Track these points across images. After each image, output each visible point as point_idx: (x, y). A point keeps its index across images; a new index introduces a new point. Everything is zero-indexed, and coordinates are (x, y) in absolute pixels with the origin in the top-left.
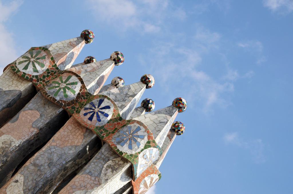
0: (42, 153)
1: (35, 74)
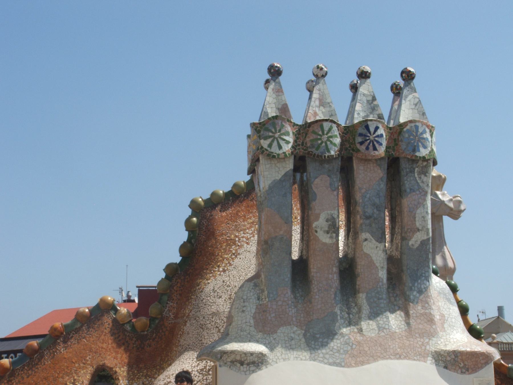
1: (290, 145)
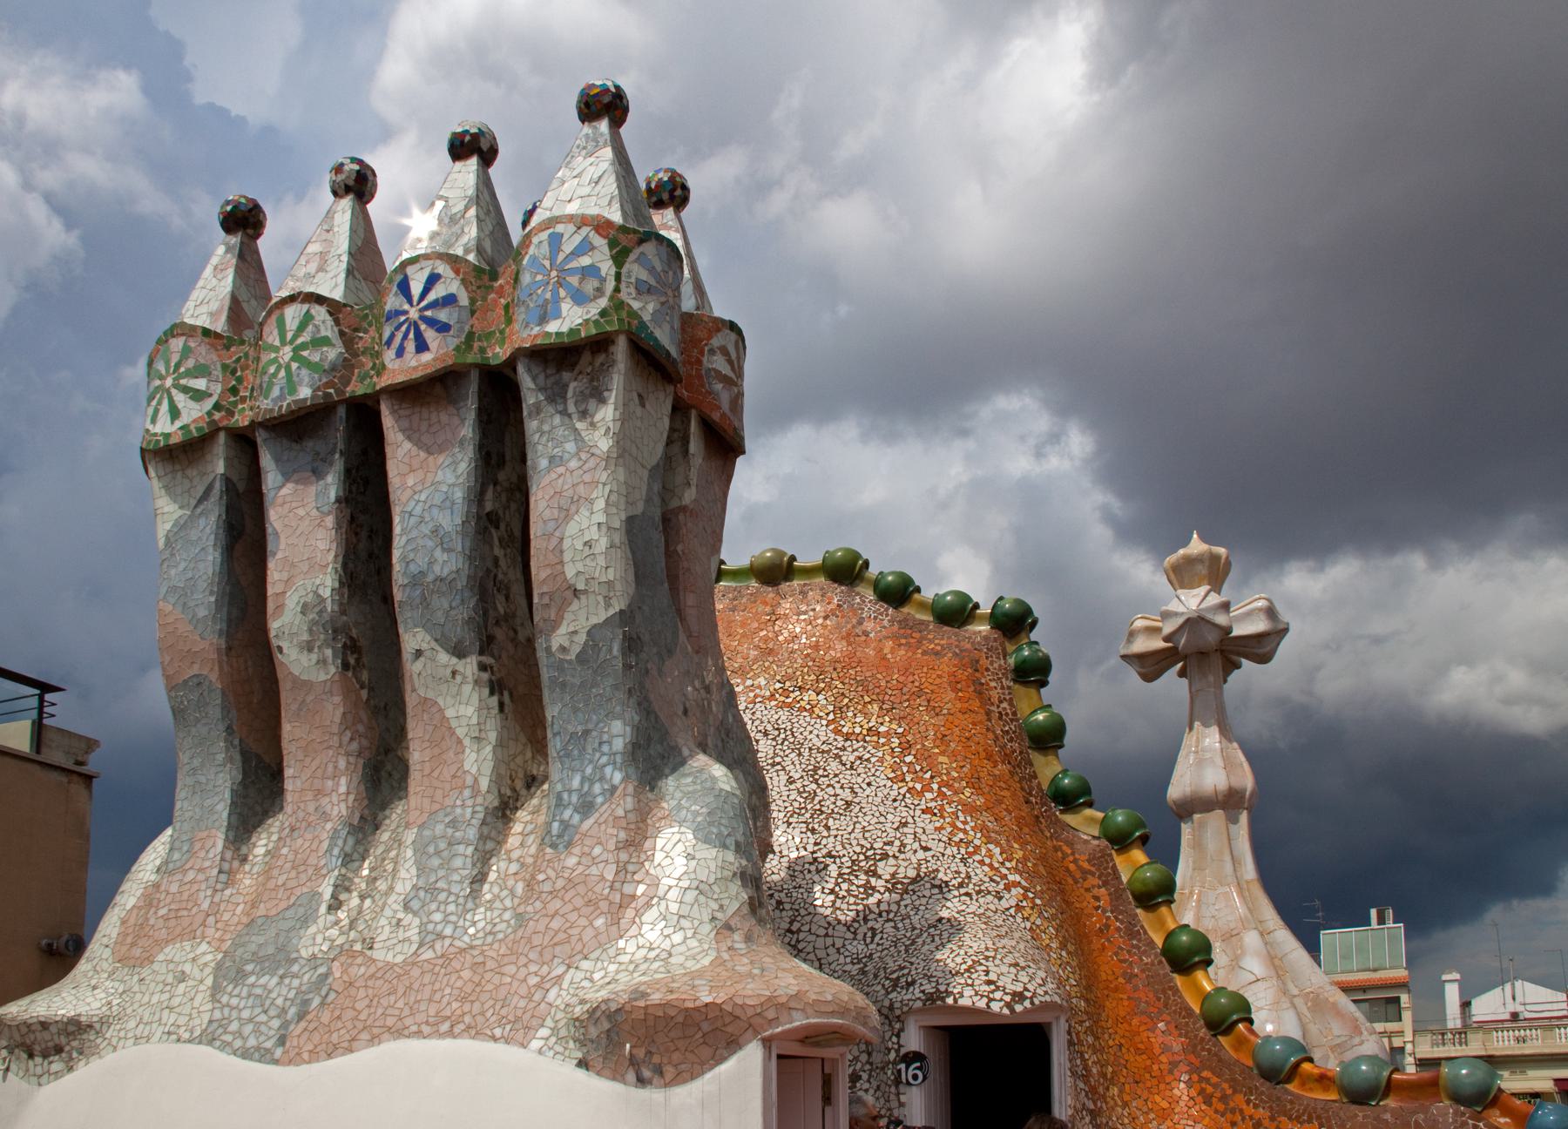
0: (404, 539)
